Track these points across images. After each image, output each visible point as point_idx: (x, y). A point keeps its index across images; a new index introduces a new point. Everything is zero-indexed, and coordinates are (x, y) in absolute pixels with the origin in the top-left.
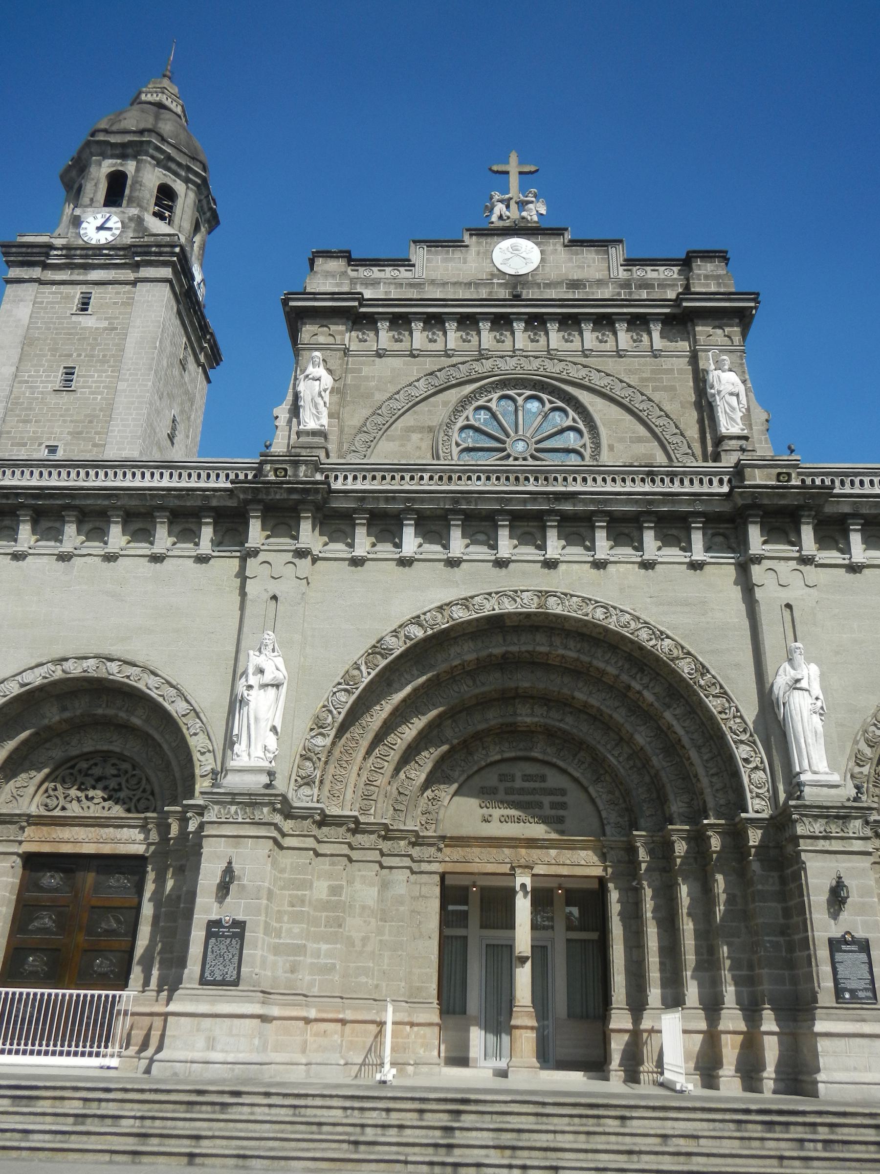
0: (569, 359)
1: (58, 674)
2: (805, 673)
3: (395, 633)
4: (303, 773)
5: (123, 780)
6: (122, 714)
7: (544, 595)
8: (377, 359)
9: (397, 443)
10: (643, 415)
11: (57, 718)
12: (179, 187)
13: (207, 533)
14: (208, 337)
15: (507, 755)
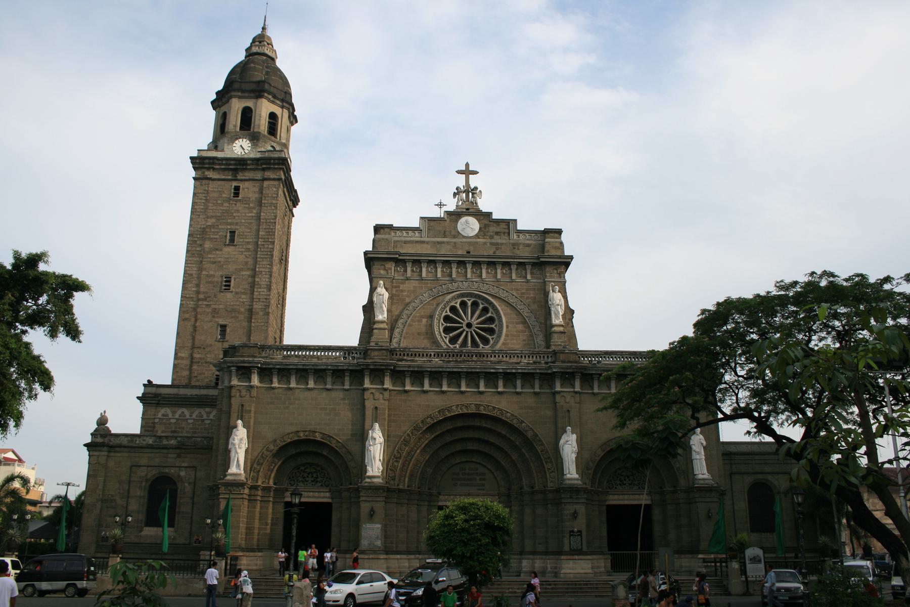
0: (490, 283)
1: (296, 438)
2: (571, 438)
3: (422, 422)
4: (391, 475)
5: (318, 474)
6: (319, 451)
7: (477, 406)
8: (407, 282)
9: (416, 323)
10: (521, 311)
11: (294, 452)
12: (277, 110)
13: (347, 380)
14: (294, 194)
15: (464, 460)
